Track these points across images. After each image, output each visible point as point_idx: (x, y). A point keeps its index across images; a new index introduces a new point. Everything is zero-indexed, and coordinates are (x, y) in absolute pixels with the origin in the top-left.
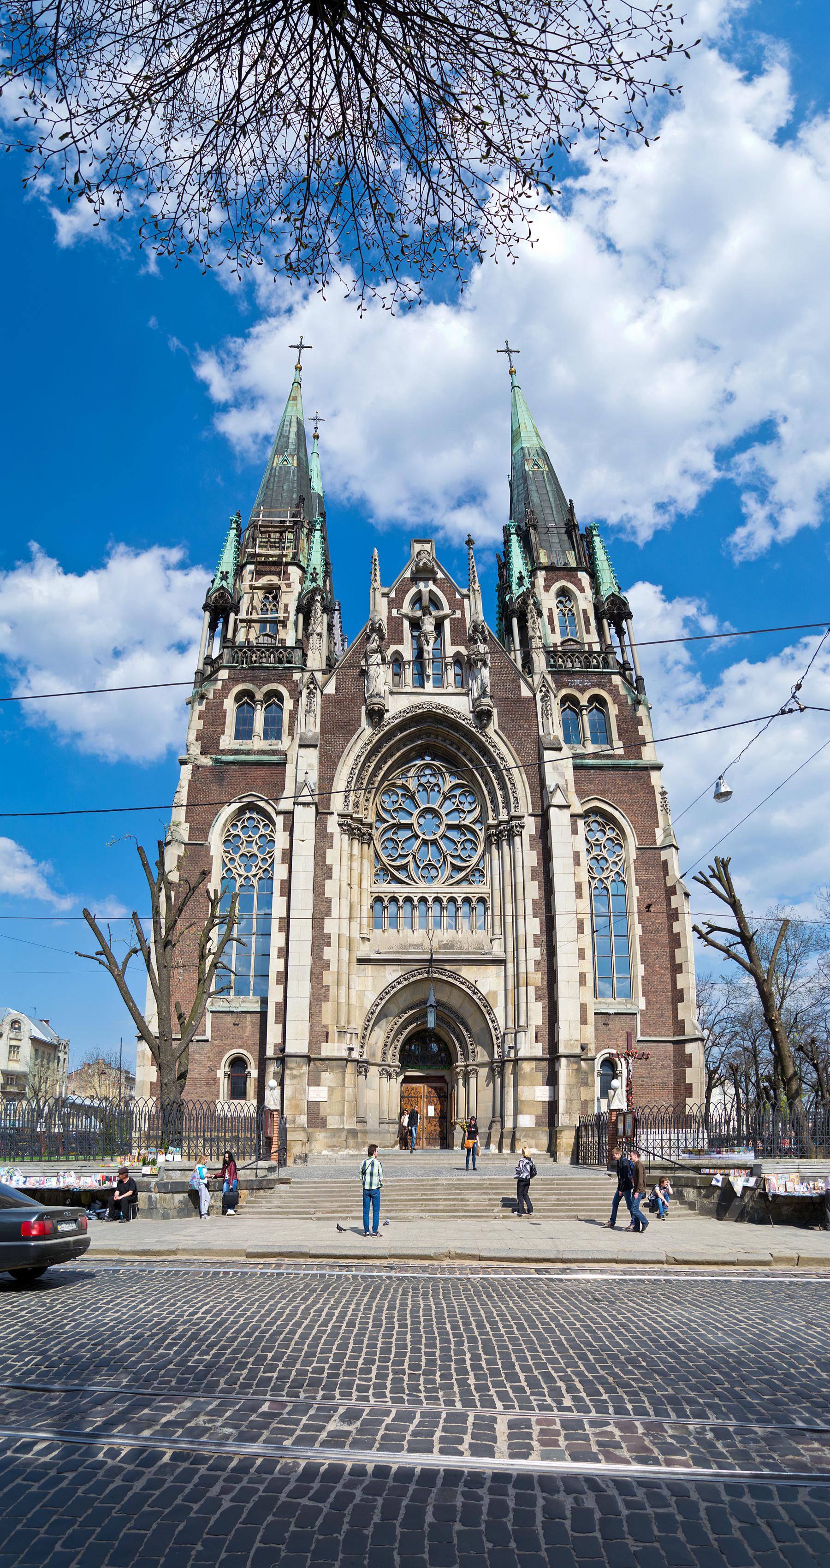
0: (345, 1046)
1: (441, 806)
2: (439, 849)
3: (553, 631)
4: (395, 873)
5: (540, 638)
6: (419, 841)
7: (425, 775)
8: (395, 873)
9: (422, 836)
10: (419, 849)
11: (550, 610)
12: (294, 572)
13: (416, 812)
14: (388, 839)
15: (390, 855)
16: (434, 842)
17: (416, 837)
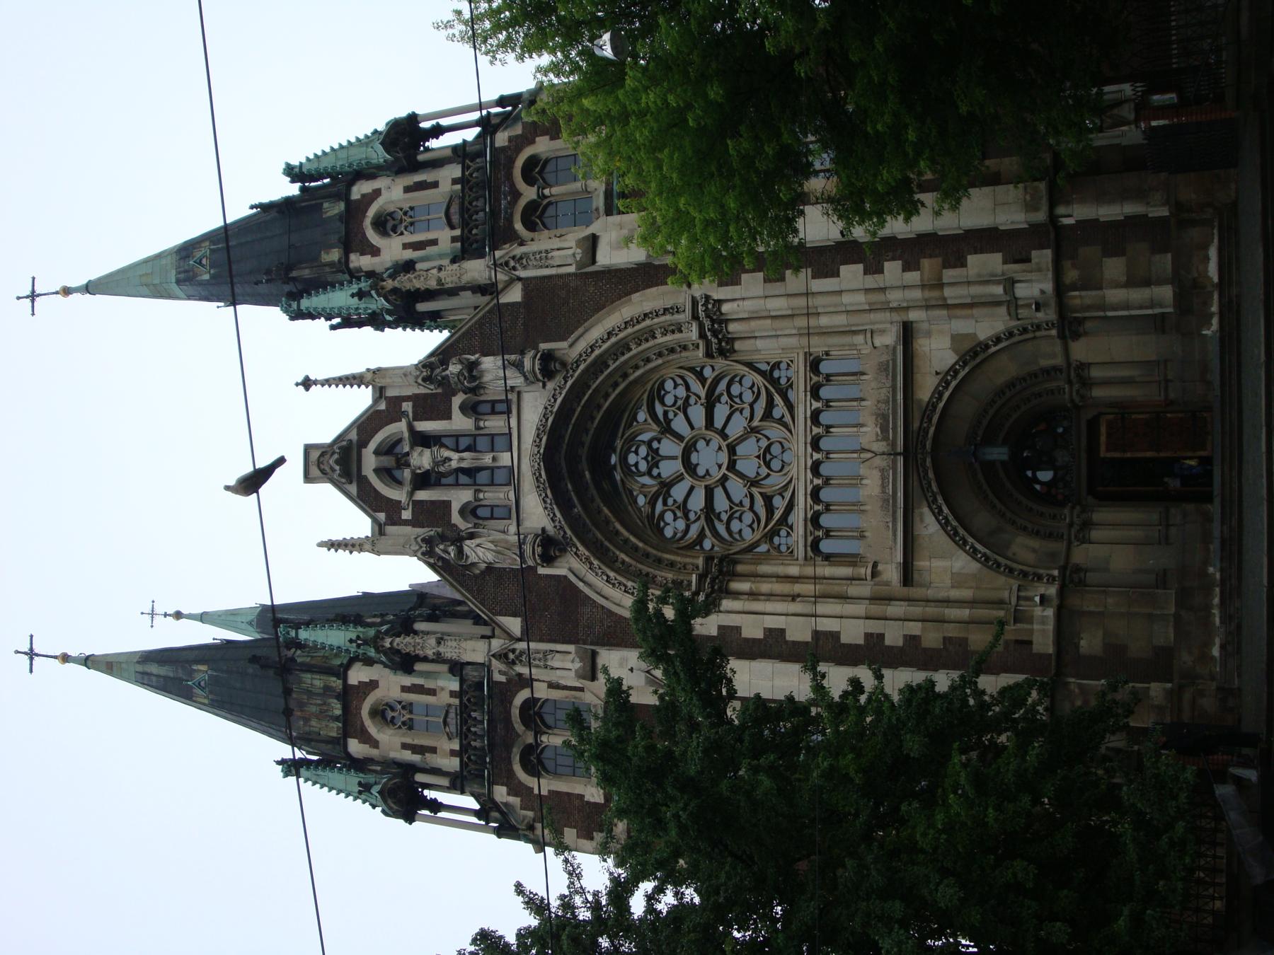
0: (1038, 611)
1: (680, 437)
2: (741, 439)
3: (434, 242)
4: (777, 515)
5: (440, 269)
6: (729, 474)
7: (636, 465)
8: (777, 515)
9: (724, 470)
10: (741, 475)
11: (406, 246)
12: (358, 675)
13: (688, 481)
14: (728, 529)
15: (750, 526)
16: (732, 449)
17: (724, 479)
